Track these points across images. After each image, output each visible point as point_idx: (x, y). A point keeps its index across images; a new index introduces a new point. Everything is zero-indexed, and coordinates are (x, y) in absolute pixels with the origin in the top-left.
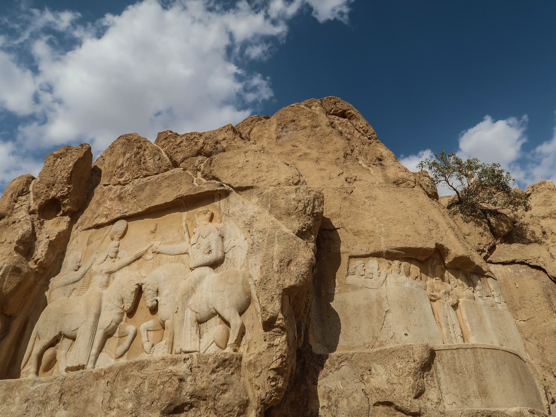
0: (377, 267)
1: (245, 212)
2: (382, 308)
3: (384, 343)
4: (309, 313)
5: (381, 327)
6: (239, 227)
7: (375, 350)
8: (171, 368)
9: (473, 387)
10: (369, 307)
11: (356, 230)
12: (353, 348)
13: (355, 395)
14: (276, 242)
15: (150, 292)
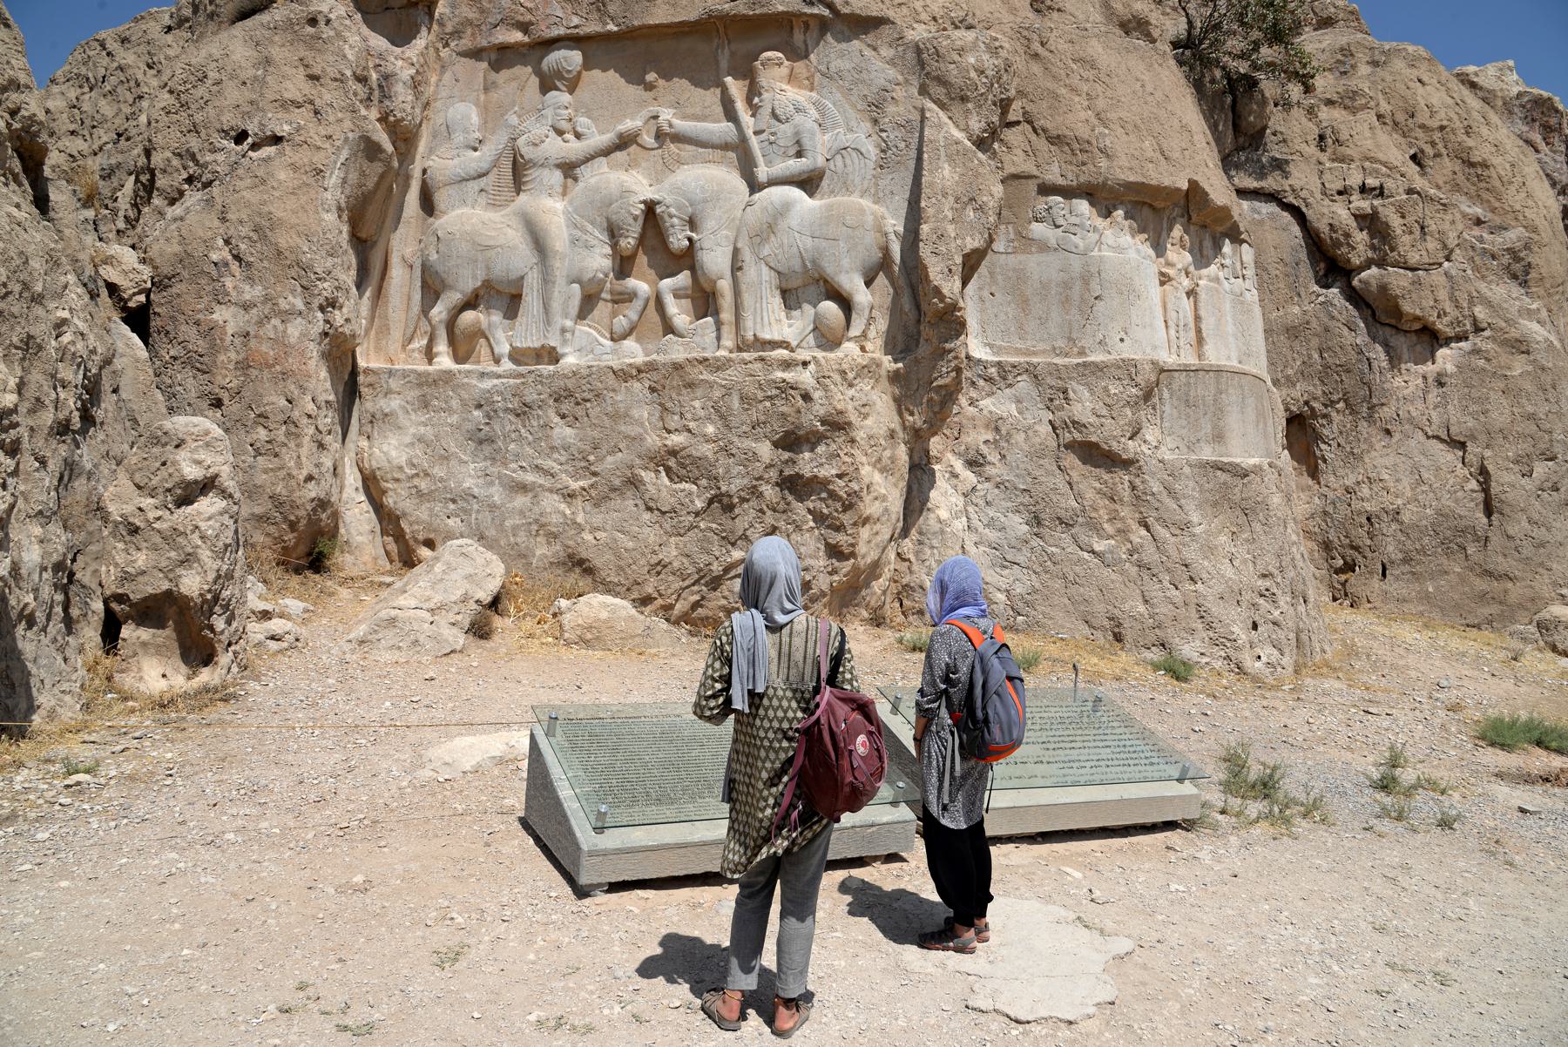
1: (864, 75)
6: (854, 106)
8: (779, 374)
9: (1207, 428)
10: (1067, 285)
11: (1055, 133)
12: (1034, 354)
13: (1037, 427)
14: (943, 158)
15: (675, 220)
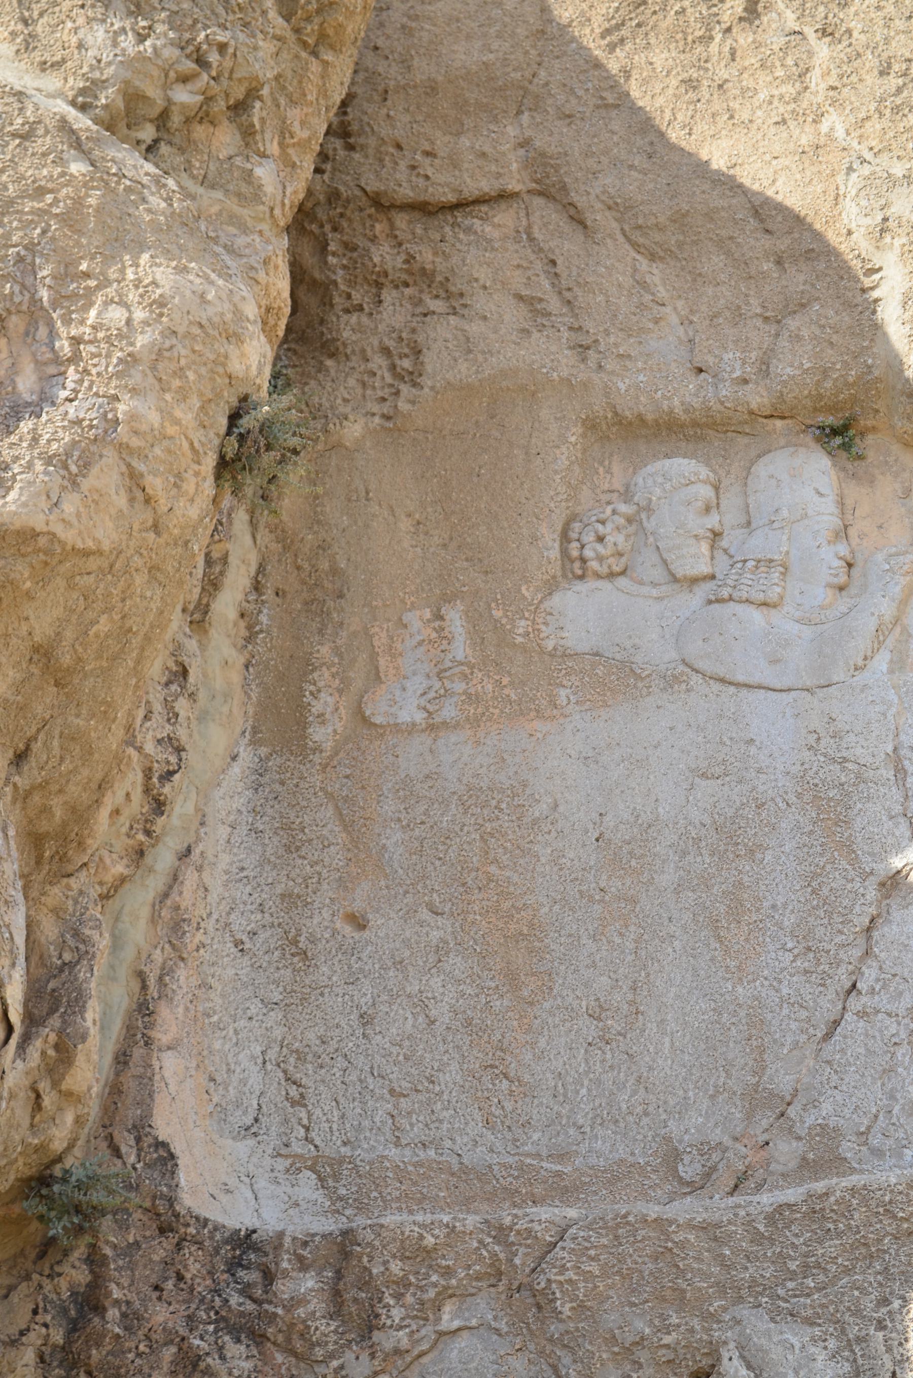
0: (826, 514)
2: (848, 848)
3: (848, 1148)
4: (175, 878)
5: (828, 1006)
7: (767, 1200)
12: (565, 1191)
